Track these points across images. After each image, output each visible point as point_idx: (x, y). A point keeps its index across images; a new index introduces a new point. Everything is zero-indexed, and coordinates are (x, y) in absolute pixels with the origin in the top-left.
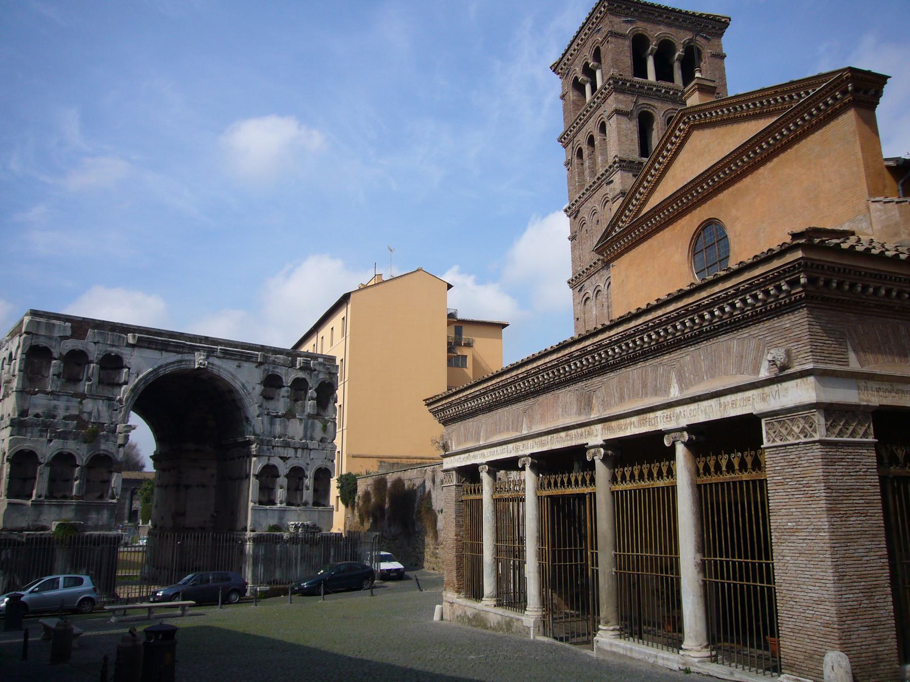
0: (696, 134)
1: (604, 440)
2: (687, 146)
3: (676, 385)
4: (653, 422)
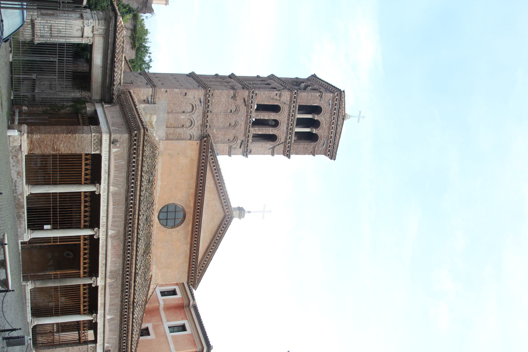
1: (98, 286)
2: (221, 209)
4: (101, 309)
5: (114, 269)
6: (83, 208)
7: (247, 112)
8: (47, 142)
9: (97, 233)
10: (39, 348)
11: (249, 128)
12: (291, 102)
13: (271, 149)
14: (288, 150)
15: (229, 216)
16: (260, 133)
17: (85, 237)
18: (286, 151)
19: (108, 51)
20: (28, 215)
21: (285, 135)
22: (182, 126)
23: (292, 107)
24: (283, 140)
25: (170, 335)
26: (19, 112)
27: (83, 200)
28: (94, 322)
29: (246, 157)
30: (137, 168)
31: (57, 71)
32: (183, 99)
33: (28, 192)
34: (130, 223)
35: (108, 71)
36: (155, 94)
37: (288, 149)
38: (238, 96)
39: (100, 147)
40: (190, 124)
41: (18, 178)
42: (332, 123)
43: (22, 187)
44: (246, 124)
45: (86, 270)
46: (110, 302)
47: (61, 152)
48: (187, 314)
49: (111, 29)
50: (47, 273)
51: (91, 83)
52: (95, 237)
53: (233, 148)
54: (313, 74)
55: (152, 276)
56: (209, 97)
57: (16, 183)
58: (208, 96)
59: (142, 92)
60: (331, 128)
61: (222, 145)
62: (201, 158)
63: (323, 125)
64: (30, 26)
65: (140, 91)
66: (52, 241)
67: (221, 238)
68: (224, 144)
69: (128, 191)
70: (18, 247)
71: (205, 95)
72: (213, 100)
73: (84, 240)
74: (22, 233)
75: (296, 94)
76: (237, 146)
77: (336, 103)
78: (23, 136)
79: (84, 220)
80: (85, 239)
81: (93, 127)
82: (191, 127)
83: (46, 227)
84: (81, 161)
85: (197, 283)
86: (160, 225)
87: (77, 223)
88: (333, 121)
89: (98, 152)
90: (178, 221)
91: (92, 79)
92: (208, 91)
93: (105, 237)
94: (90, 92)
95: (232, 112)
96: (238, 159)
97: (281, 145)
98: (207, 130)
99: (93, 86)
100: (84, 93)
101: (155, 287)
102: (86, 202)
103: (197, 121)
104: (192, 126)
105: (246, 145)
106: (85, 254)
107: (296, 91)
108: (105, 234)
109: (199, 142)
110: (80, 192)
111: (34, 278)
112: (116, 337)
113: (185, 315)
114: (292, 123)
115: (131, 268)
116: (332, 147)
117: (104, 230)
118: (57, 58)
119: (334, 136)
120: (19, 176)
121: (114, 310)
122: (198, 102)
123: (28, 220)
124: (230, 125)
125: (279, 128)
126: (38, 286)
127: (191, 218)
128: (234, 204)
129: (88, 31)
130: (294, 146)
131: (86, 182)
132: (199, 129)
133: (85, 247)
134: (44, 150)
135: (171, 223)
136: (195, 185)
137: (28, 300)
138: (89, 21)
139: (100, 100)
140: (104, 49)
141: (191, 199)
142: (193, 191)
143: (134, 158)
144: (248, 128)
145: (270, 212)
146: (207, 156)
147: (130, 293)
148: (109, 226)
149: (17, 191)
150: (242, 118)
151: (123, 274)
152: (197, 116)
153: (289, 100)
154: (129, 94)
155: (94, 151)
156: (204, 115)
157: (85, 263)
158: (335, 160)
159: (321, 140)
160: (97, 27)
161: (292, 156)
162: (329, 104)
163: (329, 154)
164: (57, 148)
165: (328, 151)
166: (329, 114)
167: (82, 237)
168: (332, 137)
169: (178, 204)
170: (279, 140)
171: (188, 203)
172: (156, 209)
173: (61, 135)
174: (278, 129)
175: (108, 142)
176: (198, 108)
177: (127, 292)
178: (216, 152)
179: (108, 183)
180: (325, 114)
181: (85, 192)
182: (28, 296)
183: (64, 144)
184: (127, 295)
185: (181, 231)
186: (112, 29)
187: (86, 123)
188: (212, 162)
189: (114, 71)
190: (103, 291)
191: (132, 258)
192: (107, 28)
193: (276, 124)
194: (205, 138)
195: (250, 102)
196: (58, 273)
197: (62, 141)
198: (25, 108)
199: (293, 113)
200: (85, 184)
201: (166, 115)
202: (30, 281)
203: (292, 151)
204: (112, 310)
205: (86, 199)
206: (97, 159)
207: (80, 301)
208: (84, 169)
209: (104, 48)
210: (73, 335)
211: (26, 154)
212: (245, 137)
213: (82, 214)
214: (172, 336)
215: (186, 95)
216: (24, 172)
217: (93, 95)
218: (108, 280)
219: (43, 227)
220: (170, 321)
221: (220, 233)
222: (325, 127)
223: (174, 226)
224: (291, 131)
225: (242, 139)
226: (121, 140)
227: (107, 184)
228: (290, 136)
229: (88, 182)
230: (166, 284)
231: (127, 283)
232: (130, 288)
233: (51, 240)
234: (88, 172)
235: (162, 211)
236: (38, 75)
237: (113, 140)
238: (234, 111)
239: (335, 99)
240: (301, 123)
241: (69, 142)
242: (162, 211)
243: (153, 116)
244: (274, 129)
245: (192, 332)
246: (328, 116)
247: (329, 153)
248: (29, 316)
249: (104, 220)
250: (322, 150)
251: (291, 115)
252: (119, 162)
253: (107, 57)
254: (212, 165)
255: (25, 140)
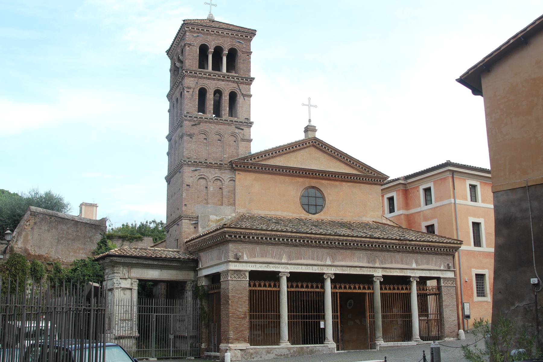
0: (313, 149)
1: (382, 275)
2: (307, 150)
3: (415, 264)
5: (366, 259)
6: (303, 289)
7: (206, 122)
8: (237, 325)
9: (329, 276)
10: (443, 334)
11: (222, 120)
12: (195, 77)
13: (245, 98)
14: (246, 80)
15: (314, 142)
16: (228, 109)
17: (333, 288)
18: (246, 81)
19: (145, 264)
20: (310, 344)
21: (229, 83)
22: (220, 190)
23: (200, 75)
24: (235, 85)
25: (434, 204)
26: (207, 352)
27: (296, 289)
28: (419, 280)
29: (252, 124)
30: (264, 235)
31: (166, 314)
32: (193, 188)
33: (287, 343)
34: (319, 242)
35: (166, 264)
36: (188, 217)
37: (245, 79)
38: (190, 132)
39: (242, 272)
40: (219, 181)
41: (273, 353)
42: (217, 33)
43: (282, 349)
44: (219, 123)
45: (366, 287)
46: (398, 263)
47: (247, 310)
48: (414, 186)
49: (123, 261)
50: (368, 325)
51: (177, 280)
52: (333, 278)
53: (243, 137)
54: (166, 53)
55: (373, 221)
56: (191, 161)
57: (278, 355)
58: (190, 163)
59: (186, 230)
60: (222, 34)
61: (240, 148)
62: (254, 170)
63: (219, 43)
64: (121, 340)
65: (185, 232)
66: (336, 320)
67: (336, 150)
68: (239, 147)
69: (287, 245)
70: (342, 353)
71: (189, 165)
72: (194, 157)
73: (336, 289)
74: (328, 349)
75: (187, 71)
76: (241, 133)
77: (197, 29)
78: (231, 348)
79: (316, 288)
80: (335, 287)
81: (222, 279)
82: (221, 180)
83: (322, 326)
84: (256, 290)
85: (382, 175)
86: (322, 213)
87: (318, 295)
88: (215, 32)
89: (247, 274)
90: (318, 194)
91: (174, 280)
92: (185, 162)
93: (333, 268)
94: (186, 282)
95: (206, 138)
96: (254, 132)
97: (240, 87)
98: (225, 164)
99: (181, 279)
100: (188, 288)
101: (385, 218)
102: (297, 287)
103: (216, 174)
104: (221, 179)
105: (241, 124)
106: (350, 288)
107: (184, 72)
108: (330, 268)
109: (237, 172)
110: (288, 292)
111: (373, 338)
112: (434, 258)
113: (414, 188)
114: (217, 76)
115: (364, 242)
116: (243, 33)
117: (326, 269)
118: (153, 314)
119: (231, 31)
120: (271, 352)
121: (407, 259)
122: (197, 173)
123: (315, 344)
124: (220, 140)
125: (223, 89)
126: (381, 335)
127: (315, 180)
128: (301, 136)
129: (126, 284)
130: (242, 73)
131: (277, 286)
132: (223, 171)
133: (343, 288)
134: (245, 327)
135: (319, 201)
136: (282, 177)
137: (395, 344)
138: (115, 282)
139: (194, 272)
140: (144, 268)
141: (296, 181)
142: (287, 179)
143: (253, 238)
144: (222, 122)
145: (309, 99)
146: (252, 164)
147: (391, 243)
148: (322, 263)
149: (286, 354)
150: (213, 127)
151: (371, 250)
152: (212, 174)
153: (194, 78)
154: (189, 243)
155: (246, 278)
156: (209, 167)
157: (359, 288)
158: (256, 30)
159: (235, 45)
160: (121, 275)
161: (252, 76)
162: (198, 36)
163: (250, 37)
164: (243, 315)
165: (246, 38)
166: (208, 36)
167: (333, 291)
168: (232, 33)
169: (301, 194)
170: (235, 89)
171: (299, 183)
172: (305, 216)
173: (230, 310)
174: (224, 90)
175: (238, 264)
176: (202, 173)
177: (389, 246)
178: (248, 155)
179: (279, 264)
180: (208, 40)
181: (288, 287)
182: (391, 344)
183: (239, 308)
184: (393, 247)
185: (328, 191)
186: (122, 259)
187: (218, 286)
188: (258, 159)
189: (165, 258)
190: (388, 270)
191: (355, 241)
192: (122, 265)
193: (218, 93)
194: (233, 166)
195: (195, 119)
196: (368, 315)
197: (236, 310)
198: (203, 346)
199: (207, 75)
200: (279, 287)
201: (209, 206)
202: (376, 342)
203: (247, 76)
204: (407, 262)
205: (295, 287)
206: (254, 275)
207: (397, 293)
208: (264, 288)
209: (142, 268)
210: (431, 301)
211: (249, 345)
212: (232, 125)
213: (309, 290)
214: (436, 201)
215: (189, 185)
216: (267, 347)
217: (189, 279)
218: (377, 265)
219: (321, 328)
220: (420, 204)
221: (331, 151)
222: (221, 41)
223: (323, 198)
224: (226, 77)
225: (234, 128)
226: (235, 250)
227: (279, 266)
228: (231, 78)
229: (277, 284)
230: (382, 207)
231: (381, 246)
232: (386, 243)
233: (335, 321)
234: (267, 284)
235: (307, 210)
236: (170, 333)
237: (235, 259)
238: (205, 136)
239: (192, 30)
240: (217, 66)
241: (237, 302)
242: (307, 210)
243: (210, 219)
244: (223, 95)
245: (432, 182)
246: (209, 38)
247: (249, 37)
248: (411, 343)
249: (316, 268)
250: (246, 44)
251: (209, 77)
252: (257, 252)
253: (151, 264)
254: (261, 159)
255: (235, 345)
